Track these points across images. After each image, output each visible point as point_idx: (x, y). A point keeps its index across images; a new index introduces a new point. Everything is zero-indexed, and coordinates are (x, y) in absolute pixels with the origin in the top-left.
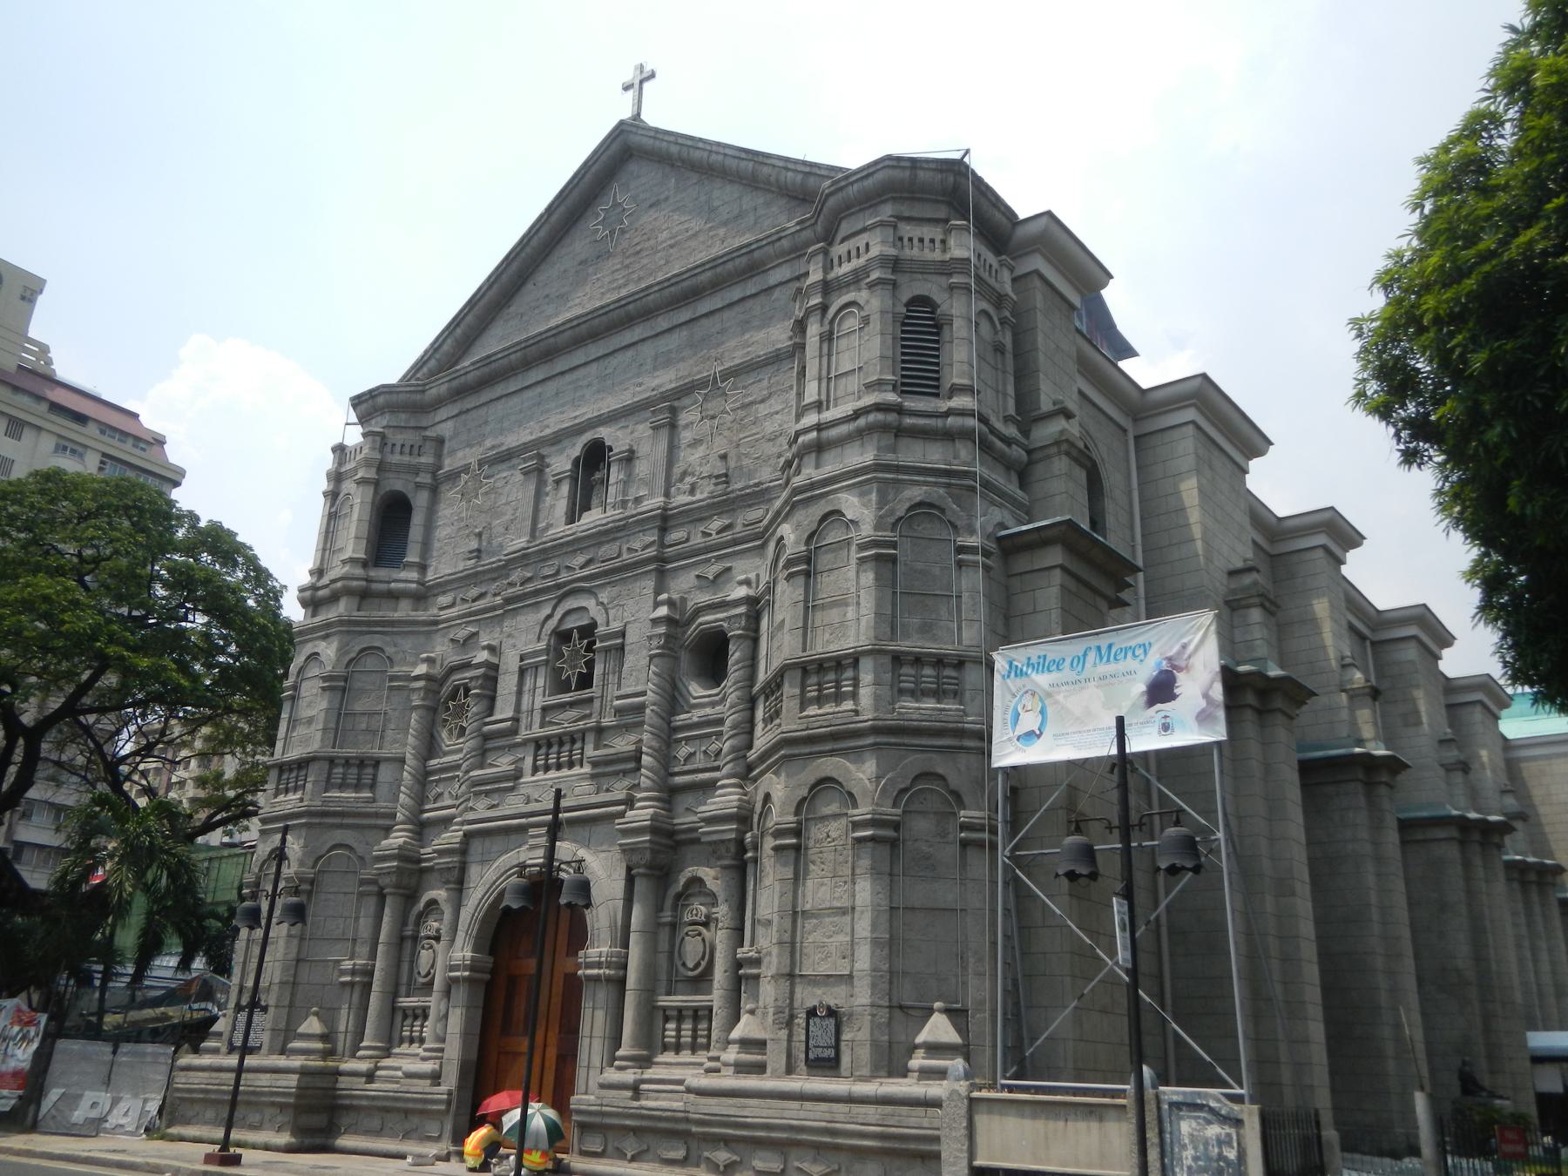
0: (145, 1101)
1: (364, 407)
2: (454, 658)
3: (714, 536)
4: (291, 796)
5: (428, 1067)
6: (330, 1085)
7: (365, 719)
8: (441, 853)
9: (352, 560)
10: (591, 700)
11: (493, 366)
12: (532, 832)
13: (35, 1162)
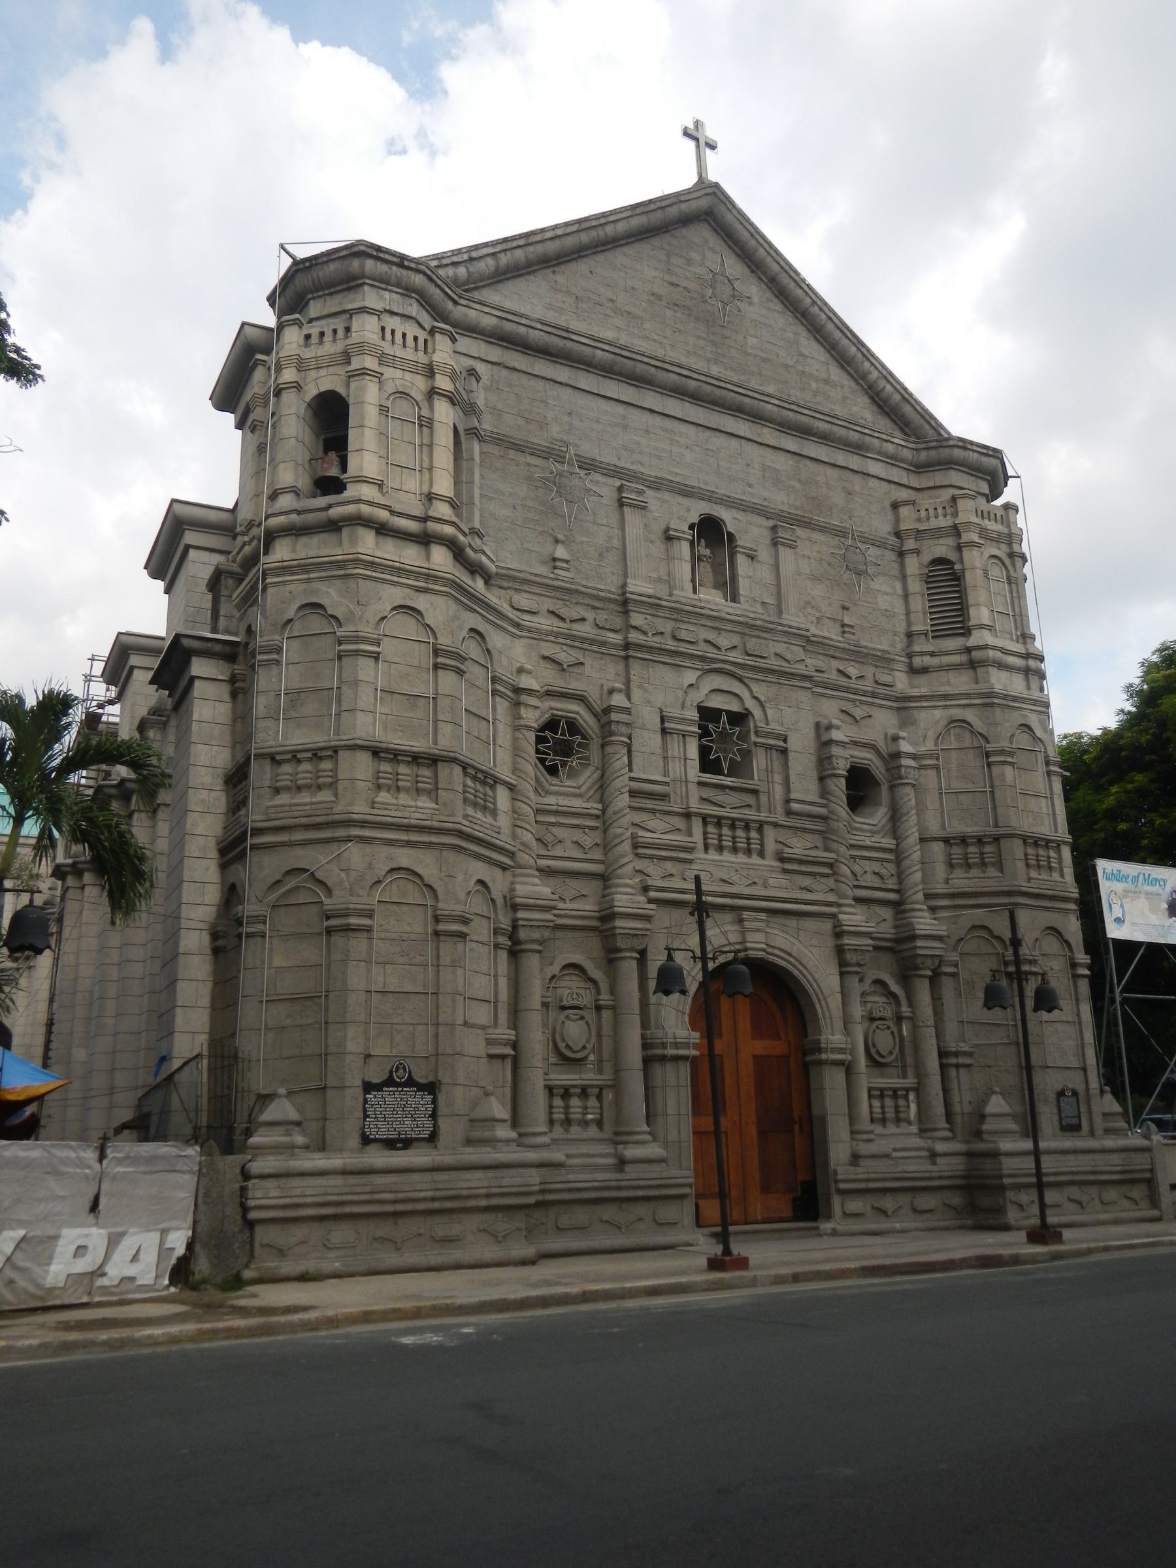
0: (164, 1232)
1: (383, 268)
3: (854, 681)
4: (404, 799)
10: (755, 792)
11: (570, 344)
12: (745, 915)
13: (629, 1304)
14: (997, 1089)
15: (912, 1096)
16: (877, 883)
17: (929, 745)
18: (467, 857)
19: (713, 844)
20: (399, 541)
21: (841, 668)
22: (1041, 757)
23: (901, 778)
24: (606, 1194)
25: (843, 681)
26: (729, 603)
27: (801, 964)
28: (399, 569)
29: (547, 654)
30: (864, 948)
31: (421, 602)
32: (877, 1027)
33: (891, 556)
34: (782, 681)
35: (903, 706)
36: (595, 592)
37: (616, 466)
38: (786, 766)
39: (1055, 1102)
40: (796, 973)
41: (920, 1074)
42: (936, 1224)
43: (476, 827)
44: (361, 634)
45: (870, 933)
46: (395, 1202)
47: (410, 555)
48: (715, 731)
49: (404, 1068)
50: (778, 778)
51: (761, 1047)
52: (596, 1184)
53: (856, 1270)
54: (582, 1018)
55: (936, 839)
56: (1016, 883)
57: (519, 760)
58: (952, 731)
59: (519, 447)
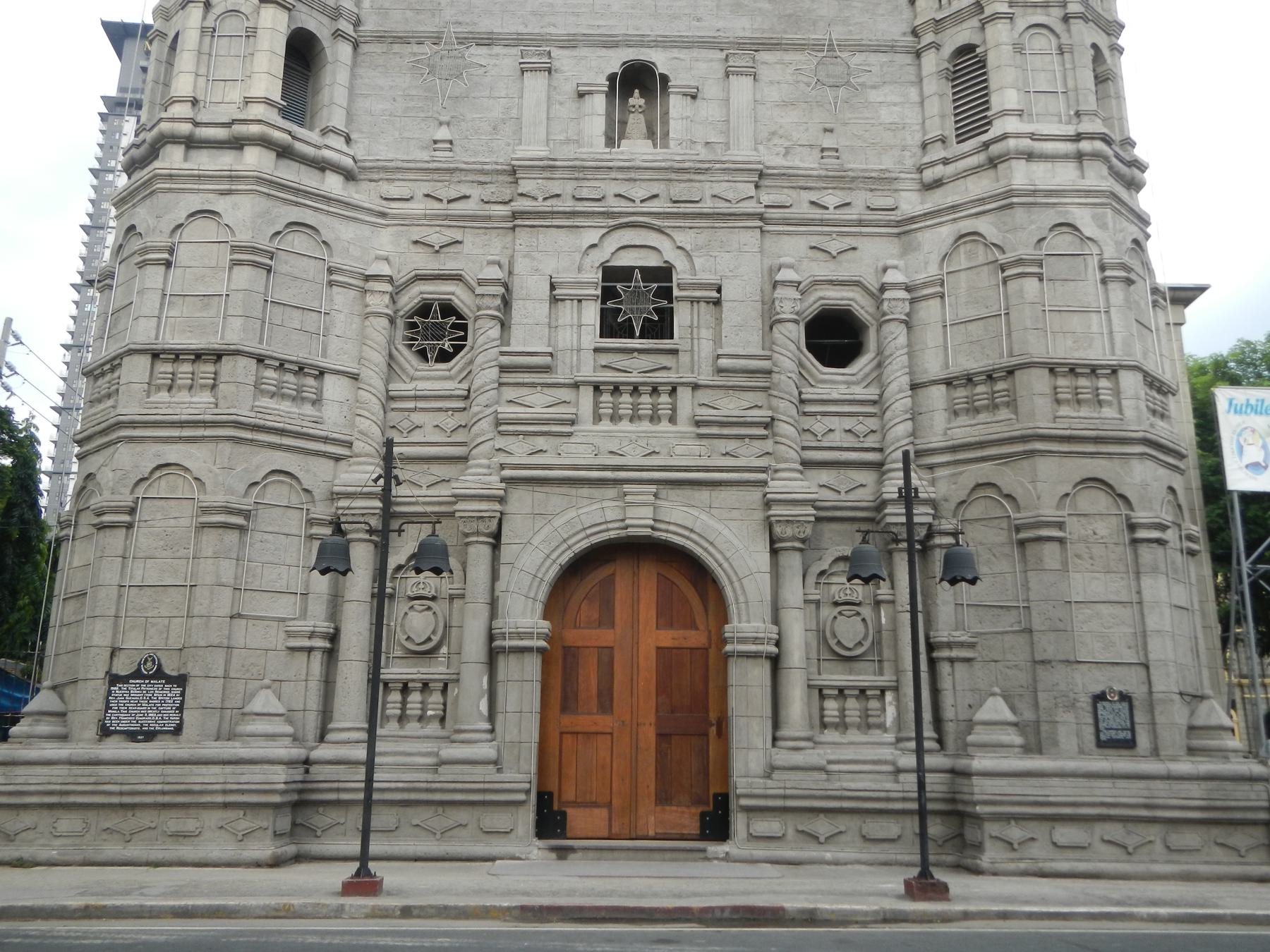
2: (424, 262)
4: (183, 396)
5: (486, 751)
6: (299, 778)
7: (296, 313)
8: (459, 498)
9: (268, 102)
10: (674, 352)
12: (627, 488)
14: (997, 690)
15: (889, 696)
16: (850, 441)
17: (933, 270)
18: (257, 449)
19: (605, 414)
20: (214, 151)
21: (814, 199)
22: (1094, 262)
23: (884, 314)
24: (413, 796)
25: (817, 213)
26: (659, 150)
27: (707, 541)
28: (199, 176)
29: (416, 238)
30: (801, 518)
31: (220, 204)
32: (840, 613)
33: (909, 59)
34: (716, 225)
35: (904, 228)
36: (479, 167)
37: (518, 34)
38: (719, 321)
39: (1090, 708)
40: (698, 551)
41: (898, 671)
42: (893, 857)
43: (267, 417)
44: (149, 244)
45: (815, 501)
46: (121, 793)
47: (224, 161)
48: (624, 290)
49: (153, 661)
50: (705, 333)
51: (667, 638)
52: (401, 785)
53: (509, 909)
54: (429, 608)
55: (935, 382)
56: (1031, 425)
57: (365, 347)
58: (962, 249)
59: (403, 40)
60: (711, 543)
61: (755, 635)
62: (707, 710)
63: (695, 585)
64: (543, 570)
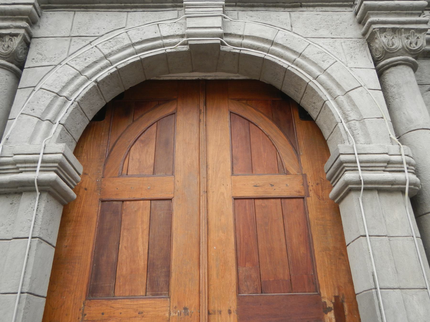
27: (294, 52)
60: (300, 55)
61: (386, 157)
62: (317, 288)
63: (277, 122)
64: (72, 87)
